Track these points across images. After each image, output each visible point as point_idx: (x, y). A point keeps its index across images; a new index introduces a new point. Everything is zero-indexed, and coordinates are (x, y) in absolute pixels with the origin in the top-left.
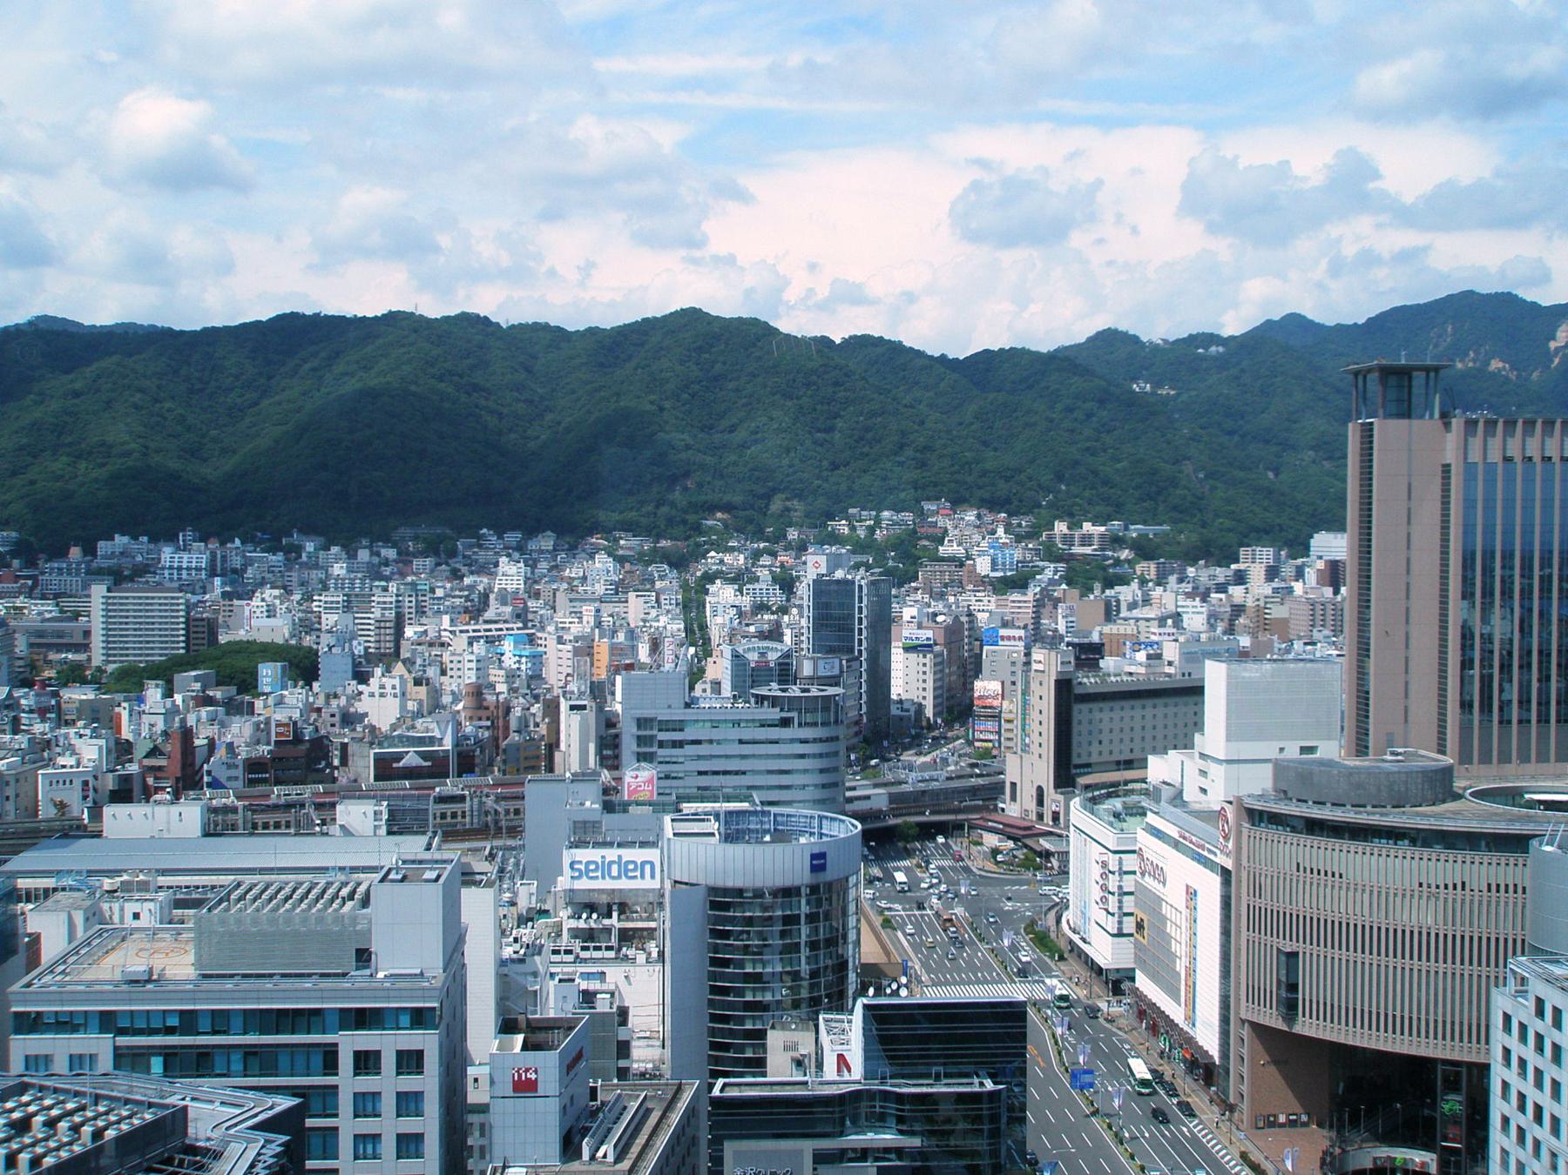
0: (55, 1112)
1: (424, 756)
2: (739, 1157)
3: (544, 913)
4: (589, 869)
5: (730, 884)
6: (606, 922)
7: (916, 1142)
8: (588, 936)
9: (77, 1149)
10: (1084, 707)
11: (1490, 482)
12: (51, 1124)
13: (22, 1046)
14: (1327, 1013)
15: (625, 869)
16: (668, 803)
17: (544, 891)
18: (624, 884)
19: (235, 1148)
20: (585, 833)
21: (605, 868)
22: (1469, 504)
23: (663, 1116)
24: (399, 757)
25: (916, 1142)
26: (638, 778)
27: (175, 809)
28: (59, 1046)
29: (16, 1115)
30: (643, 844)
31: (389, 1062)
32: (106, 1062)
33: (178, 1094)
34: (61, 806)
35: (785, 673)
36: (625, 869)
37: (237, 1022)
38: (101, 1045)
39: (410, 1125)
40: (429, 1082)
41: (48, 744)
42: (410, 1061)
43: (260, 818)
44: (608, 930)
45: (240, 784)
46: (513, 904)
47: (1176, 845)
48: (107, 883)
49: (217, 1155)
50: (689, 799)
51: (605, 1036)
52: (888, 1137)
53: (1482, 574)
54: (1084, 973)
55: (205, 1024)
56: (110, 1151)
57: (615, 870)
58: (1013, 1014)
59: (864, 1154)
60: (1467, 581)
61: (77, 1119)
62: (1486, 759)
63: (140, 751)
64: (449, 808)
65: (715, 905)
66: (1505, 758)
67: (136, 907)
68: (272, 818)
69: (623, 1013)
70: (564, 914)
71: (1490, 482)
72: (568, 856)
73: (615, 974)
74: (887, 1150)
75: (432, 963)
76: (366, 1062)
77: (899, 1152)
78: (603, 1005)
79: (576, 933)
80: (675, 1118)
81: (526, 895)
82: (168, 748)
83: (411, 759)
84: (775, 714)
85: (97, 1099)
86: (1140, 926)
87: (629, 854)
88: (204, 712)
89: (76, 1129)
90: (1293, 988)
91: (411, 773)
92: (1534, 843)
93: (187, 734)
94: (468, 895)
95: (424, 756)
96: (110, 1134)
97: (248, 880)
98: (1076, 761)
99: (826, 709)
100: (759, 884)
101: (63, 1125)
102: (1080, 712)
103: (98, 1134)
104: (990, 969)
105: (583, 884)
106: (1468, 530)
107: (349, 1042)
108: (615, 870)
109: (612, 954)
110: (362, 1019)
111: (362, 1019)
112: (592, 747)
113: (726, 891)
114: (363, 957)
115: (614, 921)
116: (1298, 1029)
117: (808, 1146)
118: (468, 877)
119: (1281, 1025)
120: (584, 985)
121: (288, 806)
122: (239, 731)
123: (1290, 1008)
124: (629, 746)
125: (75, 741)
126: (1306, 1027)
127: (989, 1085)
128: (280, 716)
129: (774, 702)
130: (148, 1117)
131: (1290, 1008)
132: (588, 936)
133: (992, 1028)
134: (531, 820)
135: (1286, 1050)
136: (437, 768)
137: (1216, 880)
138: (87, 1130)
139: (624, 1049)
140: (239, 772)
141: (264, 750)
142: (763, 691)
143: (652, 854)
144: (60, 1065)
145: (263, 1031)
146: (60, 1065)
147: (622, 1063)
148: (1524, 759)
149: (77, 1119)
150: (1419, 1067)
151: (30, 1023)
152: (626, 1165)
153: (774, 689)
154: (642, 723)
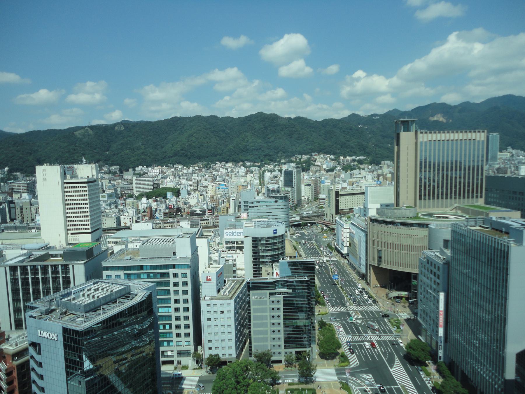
0: (104, 287)
1: (201, 211)
2: (254, 295)
3: (222, 244)
4: (230, 234)
5: (256, 236)
6: (234, 245)
7: (291, 291)
8: (230, 248)
9: (107, 294)
10: (342, 197)
11: (426, 146)
12: (102, 289)
13: (105, 273)
14: (389, 263)
15: (238, 234)
16: (249, 220)
17: (221, 239)
18: (237, 237)
19: (140, 294)
20: (232, 226)
21: (233, 234)
22: (421, 151)
23: (240, 286)
24: (195, 211)
25: (291, 291)
26: (244, 215)
27: (146, 224)
28: (113, 273)
29: (96, 287)
30: (241, 228)
31: (180, 275)
32: (122, 277)
33: (130, 283)
34: (125, 223)
35: (278, 191)
36: (238, 234)
37: (149, 267)
38: (121, 273)
39: (185, 288)
40: (189, 280)
41: (122, 211)
42: (185, 275)
43: (166, 225)
44: (234, 247)
45: (162, 218)
46: (215, 242)
47: (357, 227)
48: (131, 240)
49: (136, 295)
50: (254, 218)
51: (232, 268)
52: (282, 290)
53: (423, 165)
54: (339, 255)
55: (144, 268)
56: (114, 294)
57: (235, 234)
58: (312, 264)
59: (280, 293)
60: (421, 168)
61: (108, 288)
62: (425, 207)
63: (142, 211)
64: (203, 222)
65: (253, 241)
66: (429, 207)
67: (136, 244)
68: (168, 225)
69: (234, 265)
70: (225, 243)
71: (426, 146)
72: (225, 231)
73: (235, 256)
74: (285, 292)
75: (189, 254)
76: (175, 275)
77: (287, 293)
78: (230, 262)
79: (227, 248)
80: (242, 286)
81: (217, 240)
82: (147, 211)
83: (198, 212)
84: (274, 200)
85: (113, 284)
86: (350, 244)
87: (238, 230)
88: (155, 203)
89: (107, 290)
90: (380, 257)
91: (198, 214)
92: (429, 226)
93: (151, 208)
94: (198, 240)
95: (201, 211)
96: (114, 291)
97: (152, 238)
98: (340, 209)
99: (285, 199)
100: (262, 237)
101: (105, 289)
102: (341, 199)
103: (111, 291)
104: (318, 254)
105: (229, 237)
106: (421, 156)
107: (171, 271)
108: (235, 234)
109: (234, 252)
110: (174, 267)
111: (174, 267)
112: (237, 208)
113: (256, 238)
114: (174, 253)
115: (235, 245)
116: (381, 266)
117: (268, 292)
118: (202, 236)
119: (377, 265)
120: (227, 259)
121: (172, 222)
122: (163, 207)
123: (380, 261)
124: (243, 207)
125: (128, 210)
126: (383, 266)
127: (307, 279)
128: (170, 204)
129: (274, 197)
130: (122, 287)
131: (380, 261)
132: (230, 248)
133: (309, 266)
134: (220, 224)
135: (379, 271)
136: (204, 213)
137: (363, 234)
138: (110, 290)
139: (235, 272)
140: (162, 215)
141: (167, 211)
142: (271, 195)
143: (242, 230)
144: (113, 277)
145: (154, 269)
146: (113, 277)
147: (234, 275)
148: (434, 207)
149: (108, 288)
150: (409, 274)
151: (107, 269)
152: (230, 296)
153: (274, 195)
154: (245, 202)
